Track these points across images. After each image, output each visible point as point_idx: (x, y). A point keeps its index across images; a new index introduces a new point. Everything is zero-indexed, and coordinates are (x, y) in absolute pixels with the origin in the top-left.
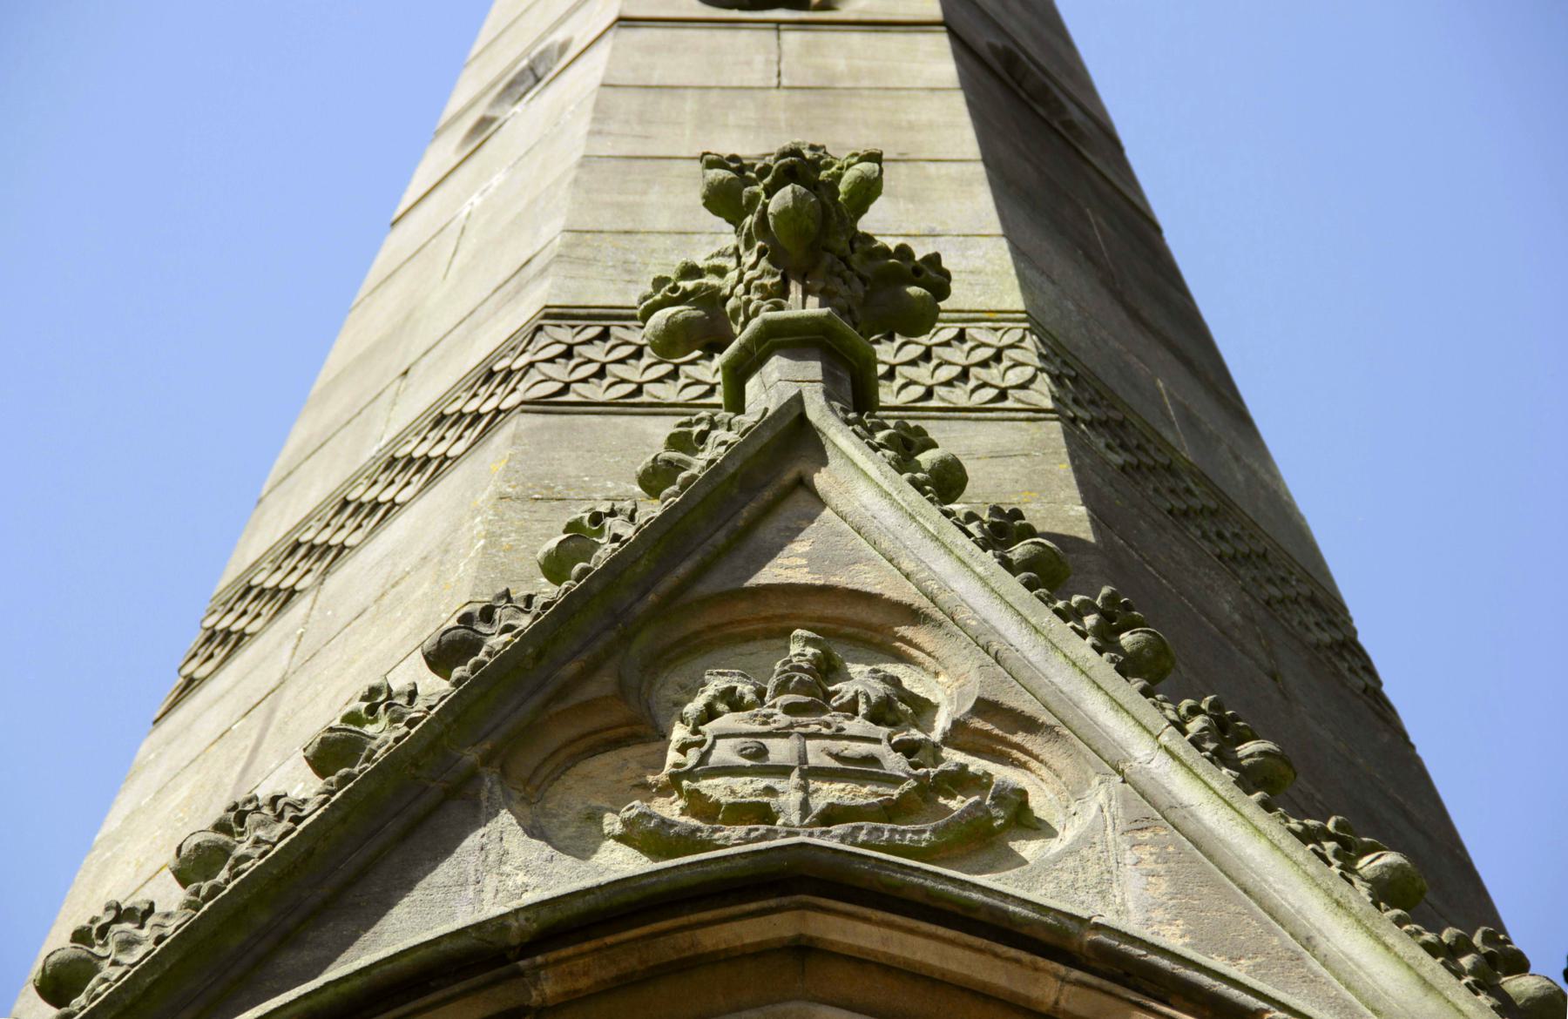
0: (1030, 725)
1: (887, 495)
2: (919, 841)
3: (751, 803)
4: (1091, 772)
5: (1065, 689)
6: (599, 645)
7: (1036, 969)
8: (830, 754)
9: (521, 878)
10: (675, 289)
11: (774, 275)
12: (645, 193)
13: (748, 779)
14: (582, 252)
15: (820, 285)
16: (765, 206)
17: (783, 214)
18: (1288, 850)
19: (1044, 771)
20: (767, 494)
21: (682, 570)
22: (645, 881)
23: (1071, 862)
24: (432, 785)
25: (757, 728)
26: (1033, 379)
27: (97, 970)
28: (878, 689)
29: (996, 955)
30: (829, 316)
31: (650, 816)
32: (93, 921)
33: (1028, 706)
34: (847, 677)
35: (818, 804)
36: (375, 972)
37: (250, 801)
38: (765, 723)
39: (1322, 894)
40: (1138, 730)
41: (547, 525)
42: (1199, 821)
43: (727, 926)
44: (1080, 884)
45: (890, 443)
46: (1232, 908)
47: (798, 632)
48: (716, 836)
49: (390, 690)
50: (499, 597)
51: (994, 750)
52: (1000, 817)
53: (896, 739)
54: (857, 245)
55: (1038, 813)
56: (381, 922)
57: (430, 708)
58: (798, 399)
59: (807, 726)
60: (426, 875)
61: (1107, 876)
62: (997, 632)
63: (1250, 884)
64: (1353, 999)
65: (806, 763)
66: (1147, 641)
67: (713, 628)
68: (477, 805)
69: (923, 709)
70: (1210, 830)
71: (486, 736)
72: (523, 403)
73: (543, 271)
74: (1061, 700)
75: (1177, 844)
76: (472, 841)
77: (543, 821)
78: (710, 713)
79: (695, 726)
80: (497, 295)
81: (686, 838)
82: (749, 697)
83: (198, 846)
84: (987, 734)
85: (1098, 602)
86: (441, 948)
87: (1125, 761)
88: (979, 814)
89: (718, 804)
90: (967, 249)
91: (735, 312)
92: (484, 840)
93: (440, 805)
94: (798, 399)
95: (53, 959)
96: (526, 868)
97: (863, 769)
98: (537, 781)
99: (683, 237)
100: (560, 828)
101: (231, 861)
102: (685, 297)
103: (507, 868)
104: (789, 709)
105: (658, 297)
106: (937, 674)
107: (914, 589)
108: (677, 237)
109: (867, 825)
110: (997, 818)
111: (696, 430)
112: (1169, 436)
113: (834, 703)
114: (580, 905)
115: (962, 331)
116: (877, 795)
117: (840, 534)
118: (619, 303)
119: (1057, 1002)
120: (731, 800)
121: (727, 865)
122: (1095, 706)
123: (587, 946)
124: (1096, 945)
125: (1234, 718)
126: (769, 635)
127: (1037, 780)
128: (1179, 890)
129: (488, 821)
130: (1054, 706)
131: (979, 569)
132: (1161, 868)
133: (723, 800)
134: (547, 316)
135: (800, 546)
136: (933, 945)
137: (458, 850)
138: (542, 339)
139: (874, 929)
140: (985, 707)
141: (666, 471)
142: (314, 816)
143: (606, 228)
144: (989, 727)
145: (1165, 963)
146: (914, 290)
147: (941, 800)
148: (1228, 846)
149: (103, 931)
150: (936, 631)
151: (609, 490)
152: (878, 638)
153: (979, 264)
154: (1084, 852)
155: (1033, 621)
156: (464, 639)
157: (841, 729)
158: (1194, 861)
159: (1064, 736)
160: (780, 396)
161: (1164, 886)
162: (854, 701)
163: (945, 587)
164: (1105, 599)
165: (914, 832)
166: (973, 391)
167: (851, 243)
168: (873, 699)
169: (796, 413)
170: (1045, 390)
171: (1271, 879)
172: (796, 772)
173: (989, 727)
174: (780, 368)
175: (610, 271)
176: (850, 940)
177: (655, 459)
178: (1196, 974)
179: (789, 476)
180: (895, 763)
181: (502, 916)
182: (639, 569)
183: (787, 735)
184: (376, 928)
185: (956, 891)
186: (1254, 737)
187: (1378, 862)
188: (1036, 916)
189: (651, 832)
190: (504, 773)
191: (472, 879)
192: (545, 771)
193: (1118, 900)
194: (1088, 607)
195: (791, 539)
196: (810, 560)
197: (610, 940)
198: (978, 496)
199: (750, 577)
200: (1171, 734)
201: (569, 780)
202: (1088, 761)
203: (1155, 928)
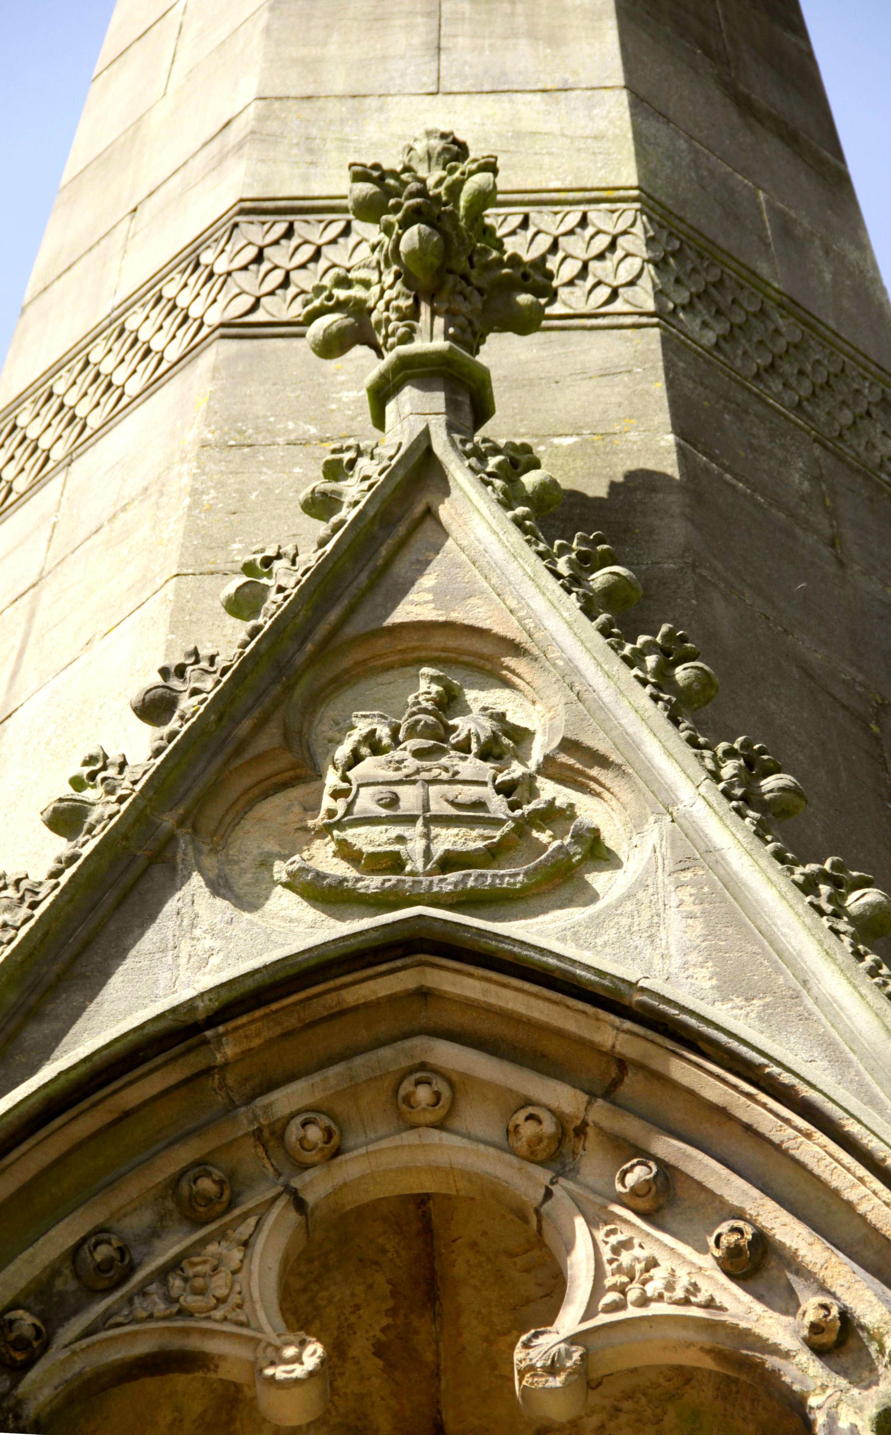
0: (604, 762)
1: (495, 533)
2: (515, 884)
3: (386, 852)
4: (648, 810)
5: (630, 731)
6: (267, 701)
7: (598, 1019)
8: (447, 801)
9: (208, 942)
10: (330, 297)
11: (408, 297)
12: (325, 44)
13: (383, 828)
14: (273, 126)
15: (445, 307)
16: (399, 237)
17: (412, 253)
18: (793, 902)
19: (614, 802)
20: (401, 530)
21: (333, 616)
22: (300, 958)
23: (629, 907)
24: (139, 853)
25: (392, 775)
26: (639, 276)
28: (486, 727)
29: (568, 1007)
30: (451, 349)
31: (306, 870)
33: (601, 745)
34: (465, 710)
35: (438, 850)
36: (96, 1058)
38: (397, 769)
39: (816, 942)
40: (684, 776)
41: (240, 478)
42: (728, 864)
43: (365, 985)
44: (636, 928)
45: (501, 472)
46: (750, 948)
47: (425, 670)
48: (359, 885)
49: (106, 757)
50: (189, 655)
51: (576, 781)
52: (577, 853)
53: (499, 779)
54: (475, 259)
55: (609, 843)
56: (102, 992)
57: (135, 783)
58: (426, 434)
59: (430, 770)
60: (135, 942)
61: (656, 919)
62: (579, 672)
63: (763, 928)
64: (837, 1037)
65: (429, 810)
66: (696, 676)
67: (358, 664)
68: (174, 869)
69: (521, 736)
70: (736, 874)
71: (181, 800)
72: (223, 325)
73: (240, 145)
74: (627, 743)
75: (712, 885)
76: (171, 906)
77: (227, 869)
78: (356, 758)
79: (344, 772)
80: (204, 153)
81: (336, 888)
82: (386, 741)
84: (570, 768)
85: (659, 639)
86: (146, 1031)
87: (674, 804)
88: (561, 856)
89: (360, 852)
90: (593, 106)
91: (379, 324)
92: (180, 904)
93: (146, 871)
94: (426, 434)
96: (212, 931)
97: (472, 814)
98: (221, 831)
99: (356, 102)
100: (240, 875)
102: (340, 306)
103: (197, 932)
104: (418, 754)
105: (317, 303)
106: (534, 703)
107: (516, 624)
108: (350, 102)
109: (475, 872)
110: (575, 854)
111: (347, 456)
112: (763, 268)
113: (453, 739)
114: (250, 984)
115: (584, 217)
116: (486, 838)
117: (459, 566)
118: (301, 193)
119: (613, 1047)
120: (371, 849)
121: (363, 938)
122: (652, 748)
123: (258, 1014)
124: (642, 1004)
125: (762, 751)
126: (405, 664)
127: (609, 809)
128: (710, 933)
129: (182, 885)
130: (621, 747)
131: (566, 614)
132: (697, 909)
133: (364, 850)
134: (243, 212)
135: (427, 581)
136: (521, 997)
137: (160, 916)
138: (239, 241)
139: (476, 983)
140: (569, 745)
141: (323, 502)
143: (293, 93)
144: (571, 761)
145: (692, 1022)
146: (524, 299)
147: (535, 834)
148: (749, 889)
150: (533, 664)
151: (290, 432)
152: (489, 666)
153: (602, 125)
154: (641, 895)
155: (606, 667)
156: (162, 698)
157: (456, 773)
158: (723, 900)
159: (629, 774)
160: (411, 433)
161: (699, 929)
162: (468, 738)
163: (540, 626)
164: (663, 637)
165: (511, 876)
166: (590, 292)
167: (470, 259)
168: (483, 739)
169: (424, 446)
170: (649, 287)
171: (779, 923)
172: (420, 822)
173: (571, 761)
174: (411, 399)
175: (295, 151)
176: (457, 991)
177: (313, 491)
178: (715, 1032)
179: (419, 509)
180: (498, 805)
181: (191, 999)
182: (299, 619)
183: (414, 782)
184: (99, 999)
185: (537, 956)
186: (778, 770)
187: (863, 901)
188: (597, 979)
189: (309, 884)
190: (195, 829)
191: (171, 945)
192: (228, 819)
193: (664, 944)
194: (649, 648)
195: (421, 572)
196: (435, 595)
197: (275, 1006)
198: (587, 425)
199: (387, 615)
200: (708, 787)
201: (247, 824)
202: (646, 801)
203: (690, 972)
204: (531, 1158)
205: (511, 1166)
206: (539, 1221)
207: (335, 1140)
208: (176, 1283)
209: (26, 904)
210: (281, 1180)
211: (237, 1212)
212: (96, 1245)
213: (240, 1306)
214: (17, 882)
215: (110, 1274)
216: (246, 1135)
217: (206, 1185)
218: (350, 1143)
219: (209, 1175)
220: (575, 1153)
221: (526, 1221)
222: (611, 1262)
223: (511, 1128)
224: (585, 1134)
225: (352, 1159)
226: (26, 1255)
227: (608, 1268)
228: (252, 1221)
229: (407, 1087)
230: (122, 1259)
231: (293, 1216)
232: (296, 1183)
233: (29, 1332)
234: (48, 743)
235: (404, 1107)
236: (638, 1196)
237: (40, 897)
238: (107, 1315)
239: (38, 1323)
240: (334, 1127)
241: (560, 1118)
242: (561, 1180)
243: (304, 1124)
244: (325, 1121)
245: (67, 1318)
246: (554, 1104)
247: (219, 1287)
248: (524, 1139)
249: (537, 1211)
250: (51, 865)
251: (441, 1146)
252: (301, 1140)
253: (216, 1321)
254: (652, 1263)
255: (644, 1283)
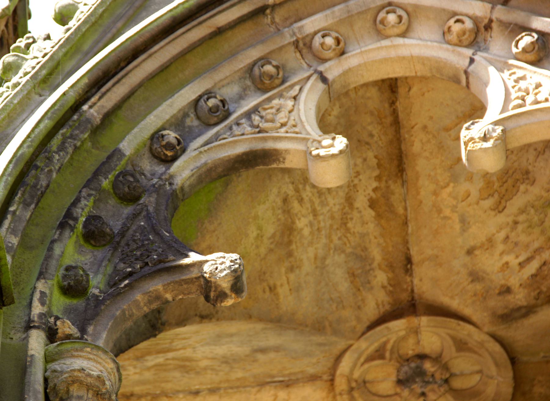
204: (460, 44)
205: (448, 50)
206: (467, 78)
207: (342, 44)
208: (256, 119)
210: (312, 68)
211: (287, 84)
212: (208, 99)
213: (295, 126)
215: (218, 114)
216: (289, 43)
217: (269, 68)
218: (350, 48)
219: (270, 63)
220: (485, 40)
221: (457, 81)
222: (513, 87)
223: (446, 29)
224: (491, 28)
225: (353, 56)
226: (168, 102)
227: (512, 91)
228: (297, 88)
229: (382, 15)
230: (224, 106)
231: (321, 86)
232: (321, 68)
233: (174, 141)
235: (381, 27)
236: (527, 52)
238: (216, 137)
239: (178, 137)
240: (340, 37)
241: (475, 20)
242: (479, 53)
243: (323, 37)
244: (335, 34)
245: (195, 138)
246: (471, 12)
247: (282, 118)
248: (455, 34)
249: (466, 72)
251: (404, 45)
252: (322, 44)
253: (282, 133)
254: (538, 86)
255: (536, 94)
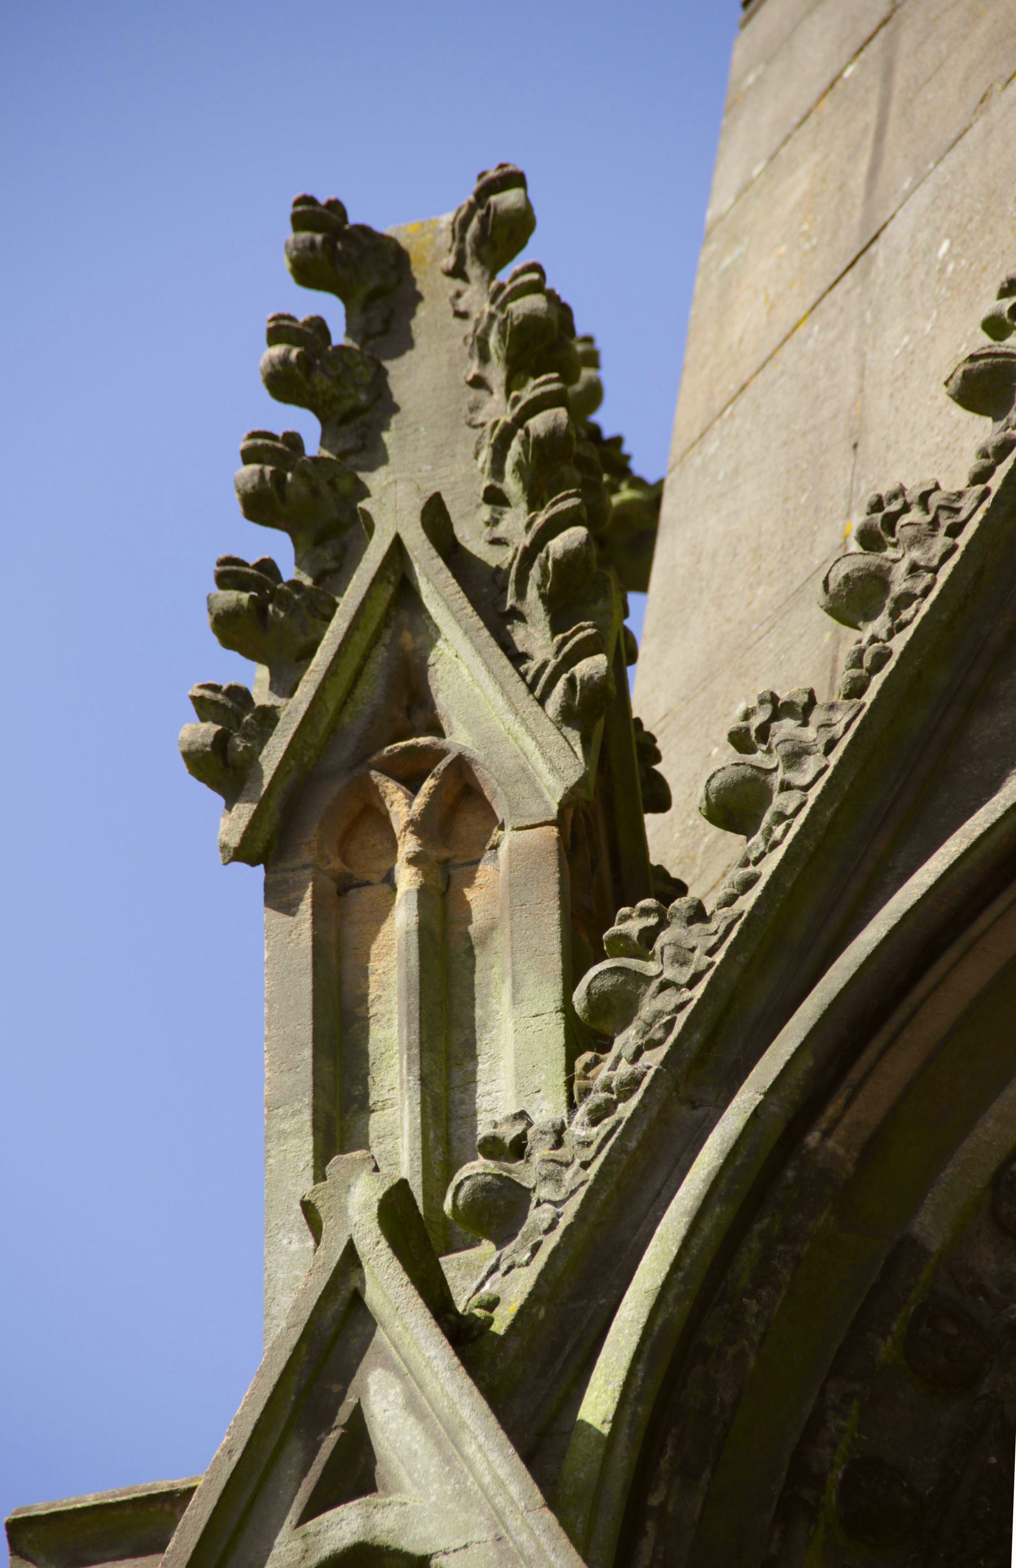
27: (765, 798)
32: (747, 715)
37: (895, 496)
83: (847, 577)
95: (715, 783)
101: (889, 604)
142: (979, 516)
149: (764, 732)
209: (942, 531)
214: (924, 498)
234: (943, 270)
237: (963, 515)
250: (971, 463)
